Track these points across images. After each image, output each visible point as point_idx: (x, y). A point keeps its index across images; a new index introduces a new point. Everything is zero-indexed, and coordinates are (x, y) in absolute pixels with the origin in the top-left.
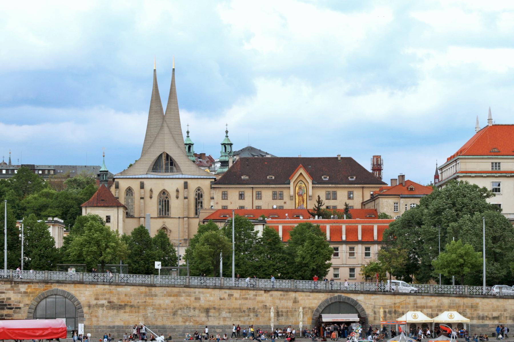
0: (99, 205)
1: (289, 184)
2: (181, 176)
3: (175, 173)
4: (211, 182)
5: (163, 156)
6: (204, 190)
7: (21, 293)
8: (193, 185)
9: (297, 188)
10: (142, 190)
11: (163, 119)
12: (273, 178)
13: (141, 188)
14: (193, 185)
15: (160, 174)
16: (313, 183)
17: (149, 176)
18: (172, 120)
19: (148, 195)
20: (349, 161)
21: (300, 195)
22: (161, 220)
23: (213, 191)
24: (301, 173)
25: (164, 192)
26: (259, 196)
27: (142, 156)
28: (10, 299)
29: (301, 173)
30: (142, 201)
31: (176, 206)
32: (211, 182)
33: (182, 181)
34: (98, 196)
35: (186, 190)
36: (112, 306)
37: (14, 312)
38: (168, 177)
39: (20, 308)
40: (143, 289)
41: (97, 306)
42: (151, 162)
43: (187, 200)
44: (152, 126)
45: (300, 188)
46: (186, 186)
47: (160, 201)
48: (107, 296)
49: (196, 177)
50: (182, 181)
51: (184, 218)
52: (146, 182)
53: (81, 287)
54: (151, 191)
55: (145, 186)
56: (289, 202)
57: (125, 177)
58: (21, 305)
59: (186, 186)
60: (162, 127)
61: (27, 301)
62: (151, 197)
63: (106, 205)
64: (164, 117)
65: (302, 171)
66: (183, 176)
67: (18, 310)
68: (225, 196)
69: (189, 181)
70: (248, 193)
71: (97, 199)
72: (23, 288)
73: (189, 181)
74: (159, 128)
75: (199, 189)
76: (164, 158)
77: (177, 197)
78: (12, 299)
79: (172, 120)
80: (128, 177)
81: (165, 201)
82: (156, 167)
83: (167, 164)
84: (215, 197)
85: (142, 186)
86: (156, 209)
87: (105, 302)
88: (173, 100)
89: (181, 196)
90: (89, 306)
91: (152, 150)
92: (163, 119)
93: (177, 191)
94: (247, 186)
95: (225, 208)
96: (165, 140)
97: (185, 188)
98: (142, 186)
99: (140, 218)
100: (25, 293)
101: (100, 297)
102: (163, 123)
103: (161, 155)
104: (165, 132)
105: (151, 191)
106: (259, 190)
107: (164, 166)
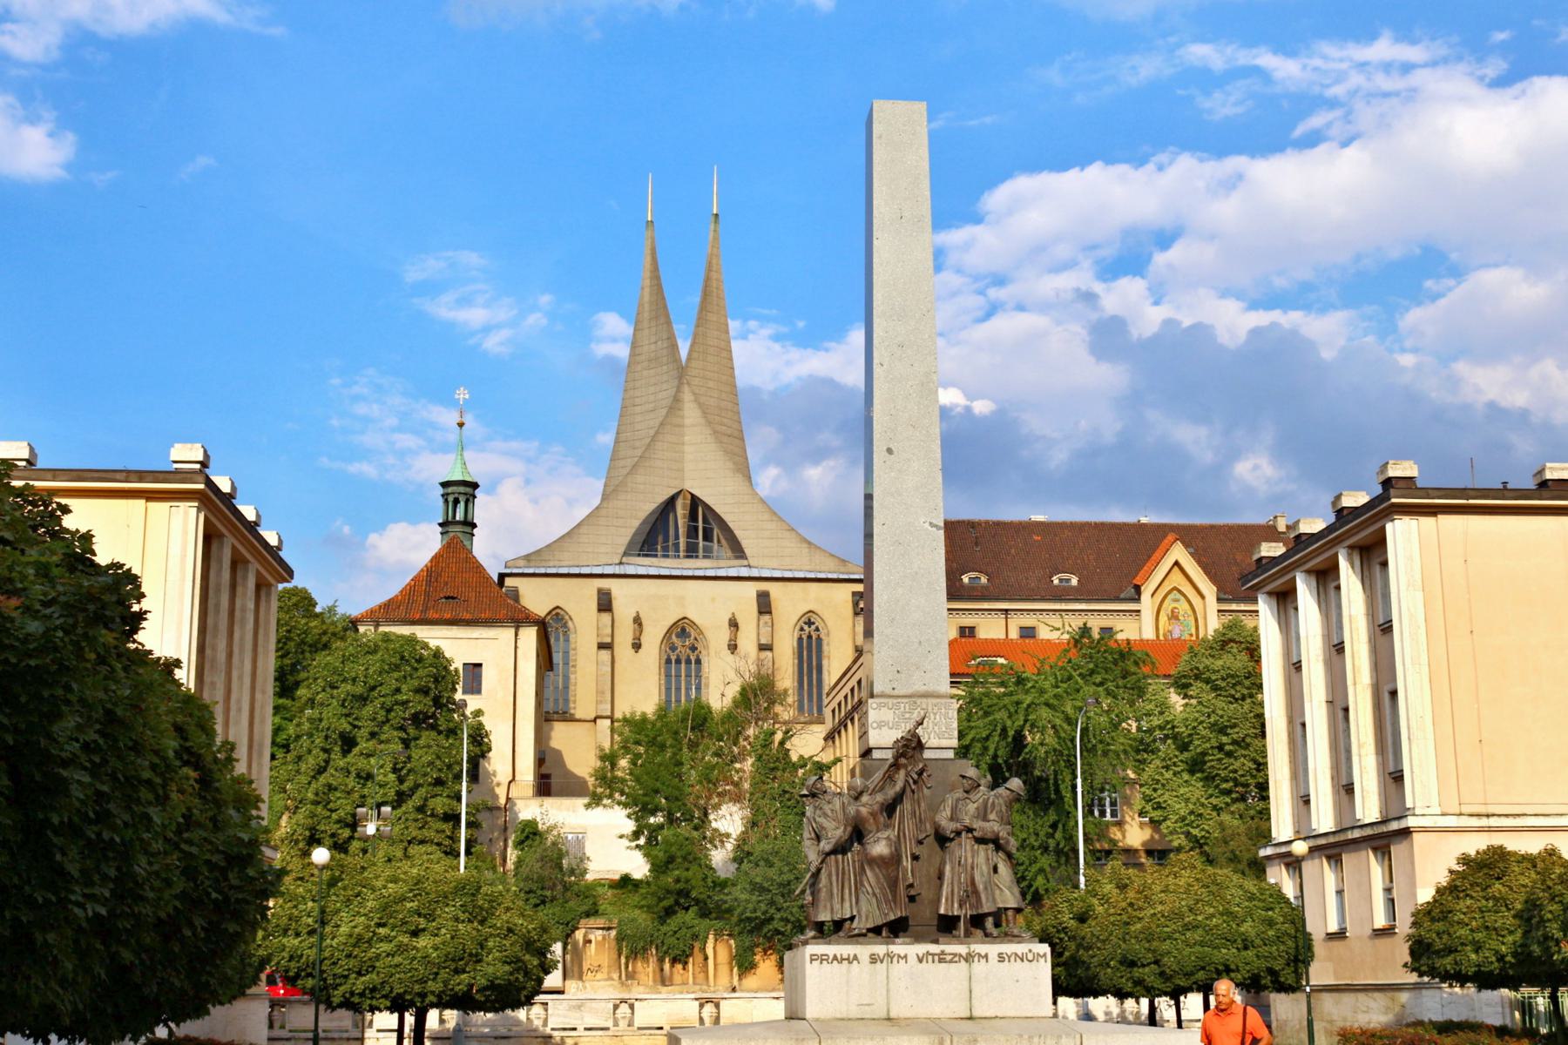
0: (432, 614)
1: (1137, 597)
2: (744, 572)
3: (722, 563)
4: (854, 594)
6: (830, 623)
8: (791, 603)
9: (1163, 618)
10: (606, 617)
11: (680, 378)
12: (1074, 581)
13: (600, 610)
14: (791, 603)
16: (1219, 600)
17: (631, 570)
18: (711, 384)
24: (1177, 563)
25: (683, 630)
27: (605, 497)
29: (1177, 563)
30: (605, 654)
32: (854, 594)
33: (751, 589)
34: (429, 583)
35: (766, 618)
38: (700, 573)
42: (636, 523)
43: (769, 654)
44: (638, 409)
45: (1174, 616)
46: (764, 605)
47: (668, 661)
49: (801, 575)
54: (638, 621)
57: (542, 571)
59: (764, 605)
60: (676, 404)
62: (637, 646)
63: (468, 616)
64: (682, 373)
65: (1179, 553)
66: (755, 573)
71: (427, 594)
74: (664, 411)
75: (809, 620)
76: (681, 510)
77: (733, 647)
79: (711, 384)
80: (553, 571)
81: (688, 661)
82: (653, 536)
83: (692, 532)
85: (605, 604)
86: (656, 691)
88: (712, 317)
89: (747, 642)
91: (640, 478)
92: (680, 378)
93: (734, 624)
94: (986, 606)
96: (687, 448)
97: (760, 613)
98: (605, 604)
99: (594, 721)
102: (679, 390)
103: (670, 503)
104: (687, 422)
105: (638, 621)
106: (1028, 621)
107: (682, 541)
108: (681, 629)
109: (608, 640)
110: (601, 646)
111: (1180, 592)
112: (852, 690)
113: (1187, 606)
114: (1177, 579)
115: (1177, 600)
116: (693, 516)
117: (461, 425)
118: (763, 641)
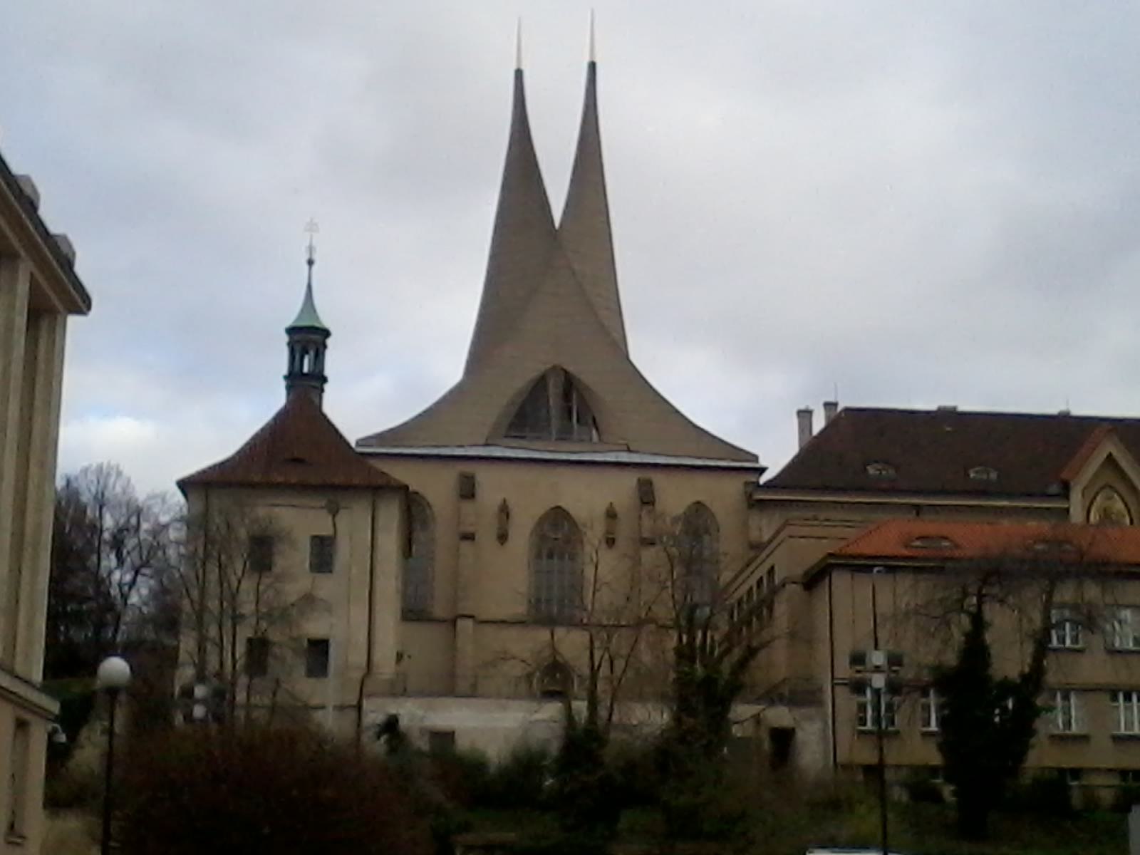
1: (1065, 493)
5: (551, 383)
10: (467, 507)
15: (538, 445)
29: (1110, 455)
30: (465, 545)
32: (747, 484)
46: (646, 496)
50: (629, 480)
52: (484, 475)
54: (505, 511)
55: (479, 491)
59: (646, 496)
62: (503, 538)
65: (1111, 447)
66: (636, 458)
73: (658, 479)
77: (611, 542)
82: (525, 417)
85: (468, 490)
94: (896, 500)
105: (505, 511)
109: (470, 529)
110: (469, 537)
111: (1111, 487)
112: (760, 582)
113: (1119, 505)
115: (1110, 498)
116: (567, 396)
117: (310, 263)
118: (646, 535)
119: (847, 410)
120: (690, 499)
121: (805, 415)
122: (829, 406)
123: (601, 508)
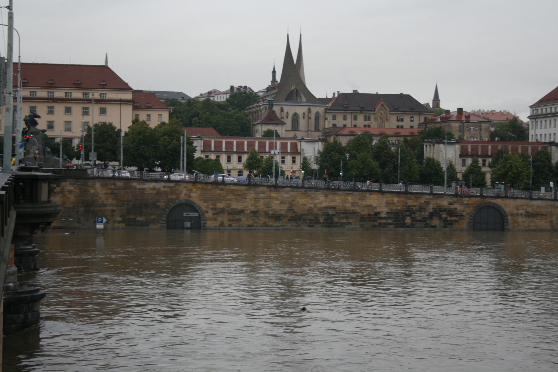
1: (374, 111)
7: (463, 204)
8: (314, 110)
19: (285, 116)
20: (408, 96)
21: (381, 118)
22: (293, 133)
23: (327, 115)
26: (355, 118)
28: (456, 209)
29: (382, 105)
31: (302, 123)
36: (529, 215)
37: (460, 219)
39: (463, 216)
40: (550, 203)
41: (518, 214)
45: (381, 114)
48: (525, 207)
50: (307, 108)
51: (308, 131)
53: (508, 201)
54: (287, 113)
56: (374, 123)
58: (464, 213)
59: (309, 111)
61: (468, 210)
62: (287, 117)
67: (462, 217)
68: (334, 118)
69: (311, 108)
70: (349, 117)
72: (466, 201)
73: (311, 108)
75: (317, 113)
76: (295, 92)
77: (304, 118)
78: (458, 209)
84: (328, 118)
85: (282, 110)
87: (523, 212)
90: (512, 215)
93: (304, 114)
95: (334, 125)
98: (282, 110)
100: (467, 204)
101: (520, 208)
105: (287, 113)
108: (295, 114)
114: (382, 107)
119: (342, 93)
120: (316, 111)
121: (334, 94)
122: (338, 92)
123: (302, 113)
